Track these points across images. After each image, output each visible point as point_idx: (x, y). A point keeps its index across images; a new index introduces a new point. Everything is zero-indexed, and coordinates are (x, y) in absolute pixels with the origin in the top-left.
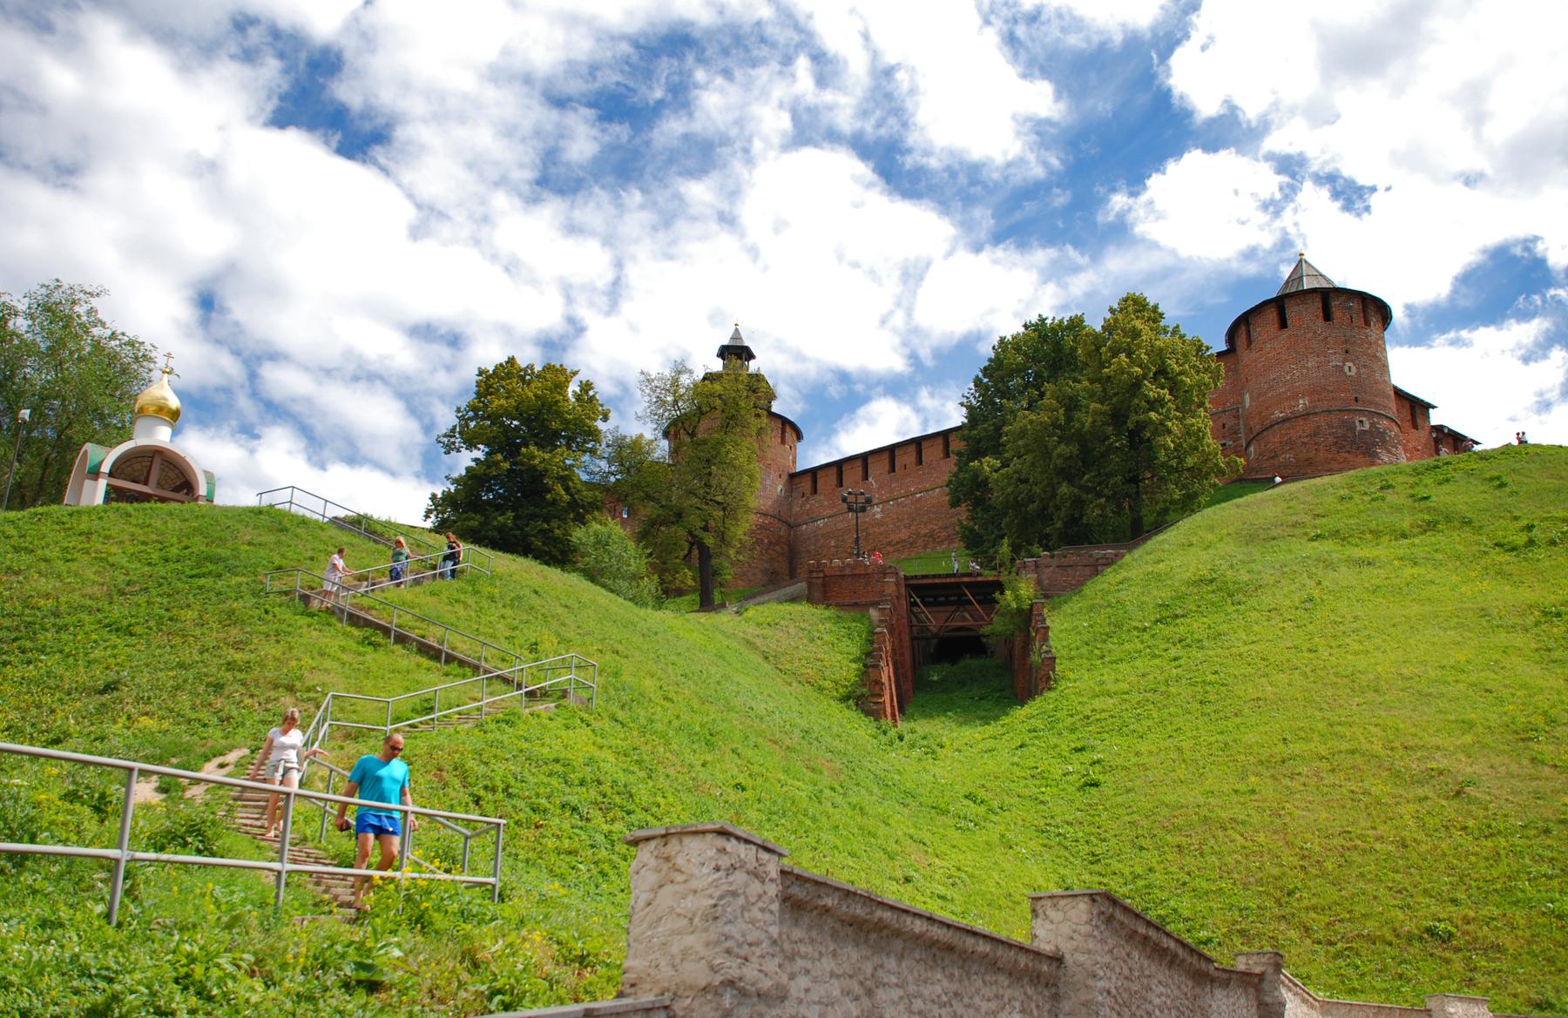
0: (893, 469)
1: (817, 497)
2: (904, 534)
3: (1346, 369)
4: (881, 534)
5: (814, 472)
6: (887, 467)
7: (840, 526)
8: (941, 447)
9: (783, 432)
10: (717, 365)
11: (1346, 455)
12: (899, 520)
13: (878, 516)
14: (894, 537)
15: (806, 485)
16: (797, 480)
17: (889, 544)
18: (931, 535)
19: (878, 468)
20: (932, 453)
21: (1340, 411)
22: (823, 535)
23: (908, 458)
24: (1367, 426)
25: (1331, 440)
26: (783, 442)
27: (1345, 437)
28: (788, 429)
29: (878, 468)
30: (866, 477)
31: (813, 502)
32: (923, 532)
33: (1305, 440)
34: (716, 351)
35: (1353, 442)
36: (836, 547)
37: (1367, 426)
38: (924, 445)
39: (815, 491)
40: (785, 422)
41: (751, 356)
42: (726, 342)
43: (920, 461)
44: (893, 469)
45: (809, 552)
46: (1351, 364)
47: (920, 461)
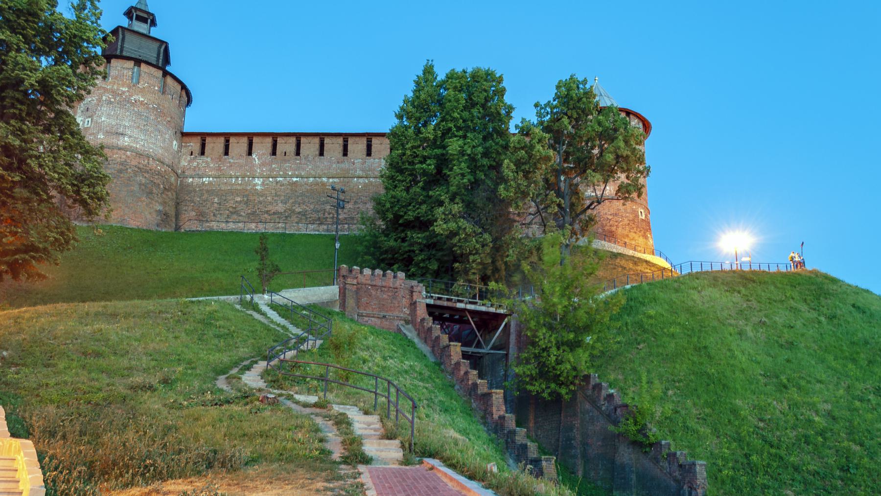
0: (274, 153)
2: (280, 207)
4: (260, 202)
5: (203, 137)
6: (270, 150)
8: (317, 146)
10: (125, 22)
11: (634, 234)
12: (276, 195)
13: (258, 188)
16: (186, 139)
17: (267, 212)
18: (304, 214)
22: (208, 191)
24: (643, 217)
27: (633, 220)
30: (250, 153)
31: (201, 160)
32: (298, 210)
33: (610, 217)
34: (125, 8)
36: (219, 204)
37: (643, 217)
39: (203, 153)
41: (153, 23)
43: (298, 153)
44: (274, 153)
45: (193, 201)
47: (298, 153)
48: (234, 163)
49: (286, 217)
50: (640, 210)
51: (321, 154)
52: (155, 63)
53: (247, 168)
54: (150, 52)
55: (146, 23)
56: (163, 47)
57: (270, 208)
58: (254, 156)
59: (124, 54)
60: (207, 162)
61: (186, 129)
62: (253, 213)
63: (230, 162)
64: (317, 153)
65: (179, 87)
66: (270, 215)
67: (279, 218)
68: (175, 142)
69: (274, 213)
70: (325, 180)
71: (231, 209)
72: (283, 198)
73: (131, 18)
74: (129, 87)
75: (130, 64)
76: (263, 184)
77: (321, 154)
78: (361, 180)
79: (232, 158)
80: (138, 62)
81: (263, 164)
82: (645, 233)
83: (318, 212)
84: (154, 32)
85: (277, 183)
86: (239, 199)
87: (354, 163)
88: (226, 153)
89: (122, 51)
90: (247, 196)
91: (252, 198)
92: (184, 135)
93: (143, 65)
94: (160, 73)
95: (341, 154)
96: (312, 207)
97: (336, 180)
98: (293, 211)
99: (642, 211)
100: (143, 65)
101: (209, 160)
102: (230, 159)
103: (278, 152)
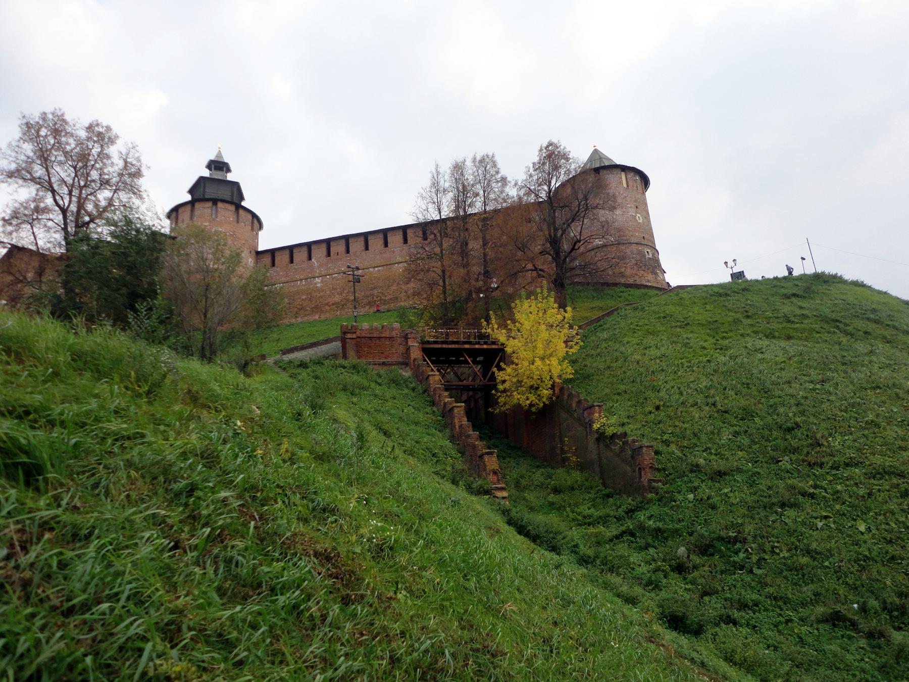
0: (329, 254)
1: (274, 268)
2: (337, 299)
3: (637, 218)
4: (321, 297)
5: (272, 252)
7: (292, 290)
9: (253, 223)
10: (206, 173)
11: (642, 272)
13: (319, 285)
14: (331, 300)
15: (267, 260)
16: (260, 256)
17: (327, 304)
19: (319, 254)
20: (395, 240)
21: (637, 244)
23: (340, 248)
24: (651, 256)
25: (633, 262)
26: (252, 229)
27: (640, 260)
28: (255, 221)
29: (319, 254)
30: (310, 258)
31: (272, 272)
34: (206, 163)
35: (645, 265)
36: (289, 303)
37: (651, 256)
38: (351, 240)
39: (273, 264)
40: (254, 216)
41: (229, 170)
42: (213, 158)
44: (329, 254)
46: (638, 215)
47: (348, 251)
48: (298, 269)
49: (343, 306)
50: (646, 250)
51: (367, 248)
52: (229, 199)
53: (308, 270)
54: (225, 193)
55: (222, 170)
56: (236, 187)
57: (329, 300)
58: (313, 260)
59: (207, 197)
60: (277, 272)
61: (260, 249)
62: (316, 307)
63: (295, 269)
64: (363, 248)
65: (250, 217)
66: (330, 306)
67: (337, 307)
68: (250, 260)
69: (333, 304)
70: (371, 270)
71: (298, 307)
72: (339, 290)
73: (210, 169)
74: (210, 222)
75: (210, 204)
76: (322, 282)
77: (367, 248)
78: (401, 265)
79: (297, 265)
80: (215, 201)
81: (320, 266)
82: (653, 270)
83: (368, 297)
84: (230, 177)
85: (333, 278)
86: (304, 297)
87: (394, 252)
88: (292, 261)
89: (204, 195)
90: (310, 293)
91: (314, 294)
92: (259, 254)
93: (220, 205)
94: (233, 208)
95: (383, 246)
96: (363, 293)
97: (380, 268)
98: (348, 300)
99: (649, 251)
100: (220, 205)
101: (278, 269)
102: (294, 266)
103: (332, 254)
